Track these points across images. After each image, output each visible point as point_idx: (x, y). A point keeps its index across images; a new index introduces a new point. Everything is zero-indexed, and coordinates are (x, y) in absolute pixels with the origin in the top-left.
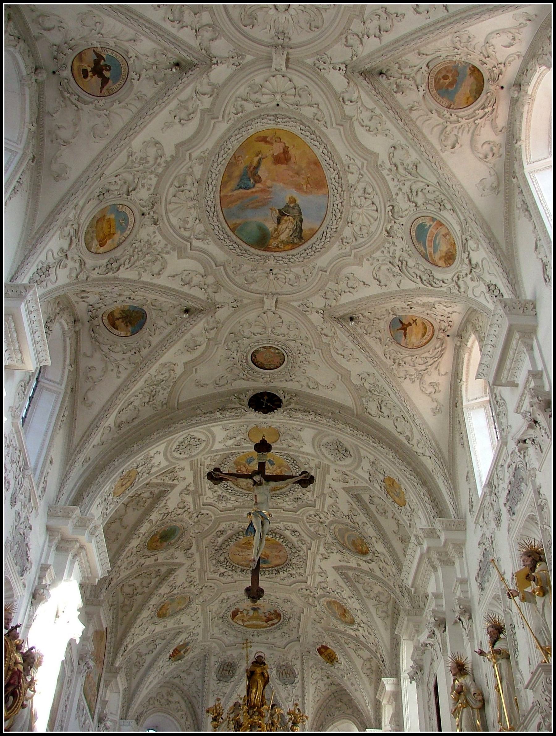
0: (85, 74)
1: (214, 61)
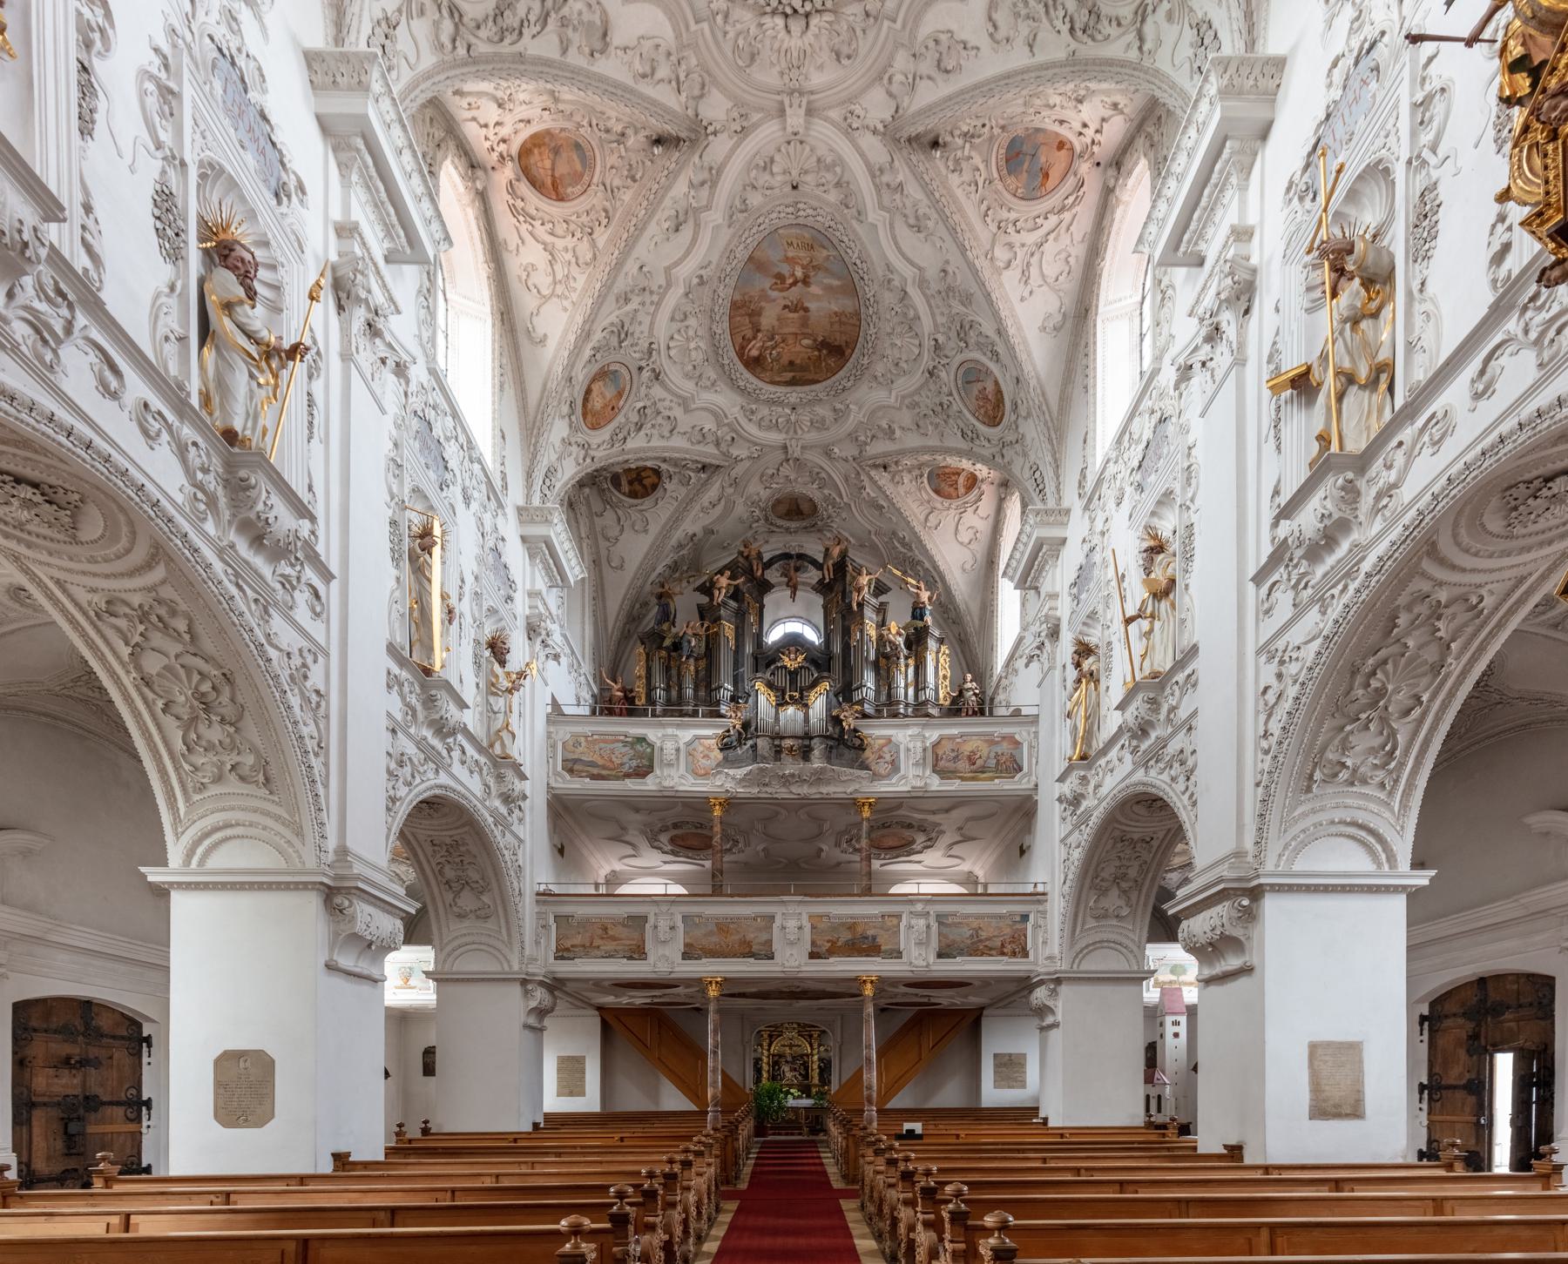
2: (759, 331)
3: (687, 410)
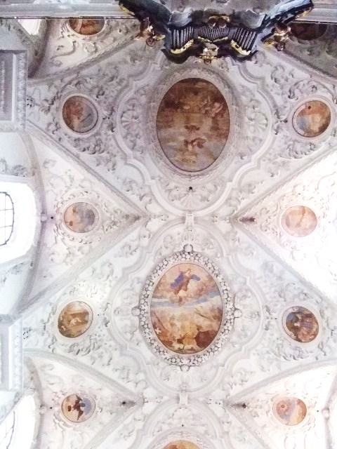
0: (69, 409)
1: (146, 400)
2: (213, 118)
3: (262, 79)
